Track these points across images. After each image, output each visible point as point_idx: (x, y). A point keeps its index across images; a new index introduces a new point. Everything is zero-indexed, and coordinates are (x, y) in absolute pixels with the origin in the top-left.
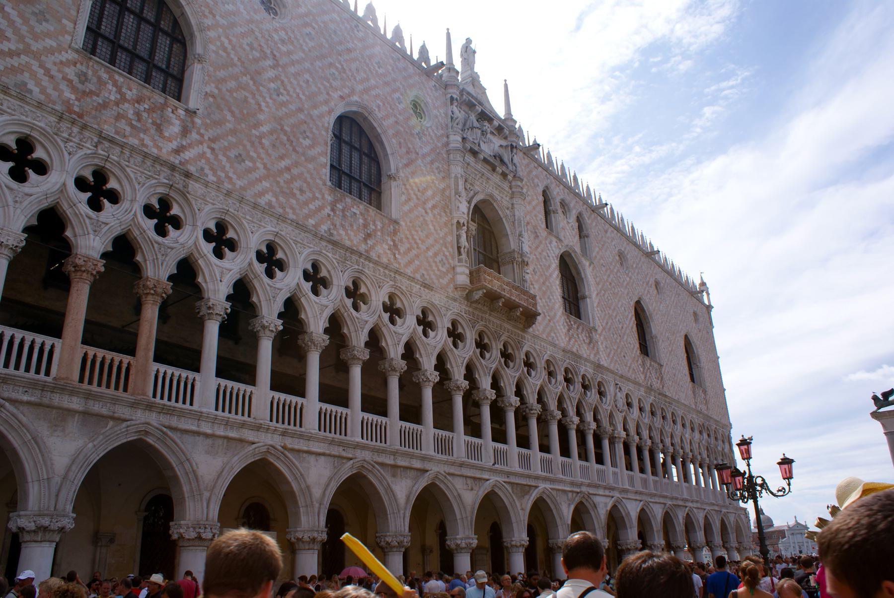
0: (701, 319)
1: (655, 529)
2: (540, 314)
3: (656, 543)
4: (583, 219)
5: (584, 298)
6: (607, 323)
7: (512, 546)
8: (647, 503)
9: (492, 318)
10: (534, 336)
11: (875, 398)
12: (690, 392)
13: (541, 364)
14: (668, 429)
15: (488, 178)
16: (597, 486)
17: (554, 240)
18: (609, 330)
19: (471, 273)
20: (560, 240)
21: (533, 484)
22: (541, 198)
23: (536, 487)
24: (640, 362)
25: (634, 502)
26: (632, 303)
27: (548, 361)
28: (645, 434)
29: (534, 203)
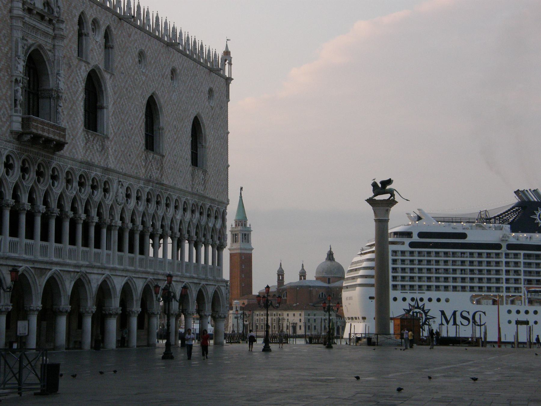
0: (216, 95)
1: (135, 298)
2: (67, 143)
3: (133, 310)
4: (111, 31)
5: (102, 108)
6: (119, 128)
7: (31, 310)
8: (131, 279)
9: (32, 149)
10: (61, 156)
11: (375, 185)
12: (189, 176)
13: (62, 177)
14: (160, 213)
15: (38, 29)
16: (93, 267)
17: (83, 64)
18: (120, 134)
19: (23, 119)
20: (88, 63)
21: (49, 267)
22: (76, 27)
23: (50, 270)
24: (144, 156)
25: (120, 278)
26: (145, 102)
27: (68, 173)
28: (139, 220)
29: (70, 35)
